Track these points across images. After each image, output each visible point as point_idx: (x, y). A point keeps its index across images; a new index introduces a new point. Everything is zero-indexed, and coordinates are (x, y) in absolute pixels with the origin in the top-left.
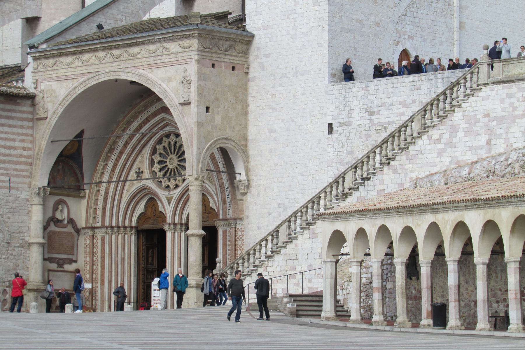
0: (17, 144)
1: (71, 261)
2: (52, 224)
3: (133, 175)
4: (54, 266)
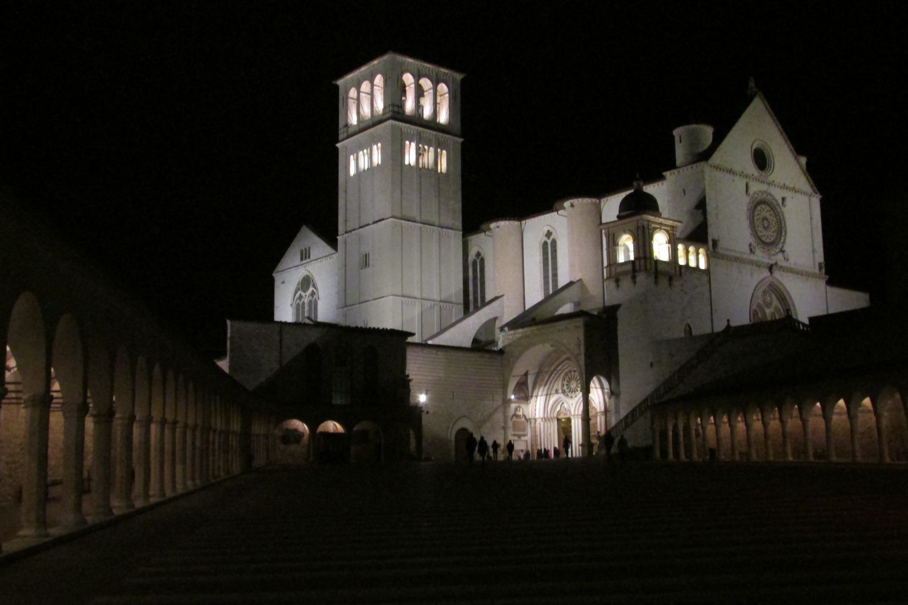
1: (524, 435)
3: (553, 391)
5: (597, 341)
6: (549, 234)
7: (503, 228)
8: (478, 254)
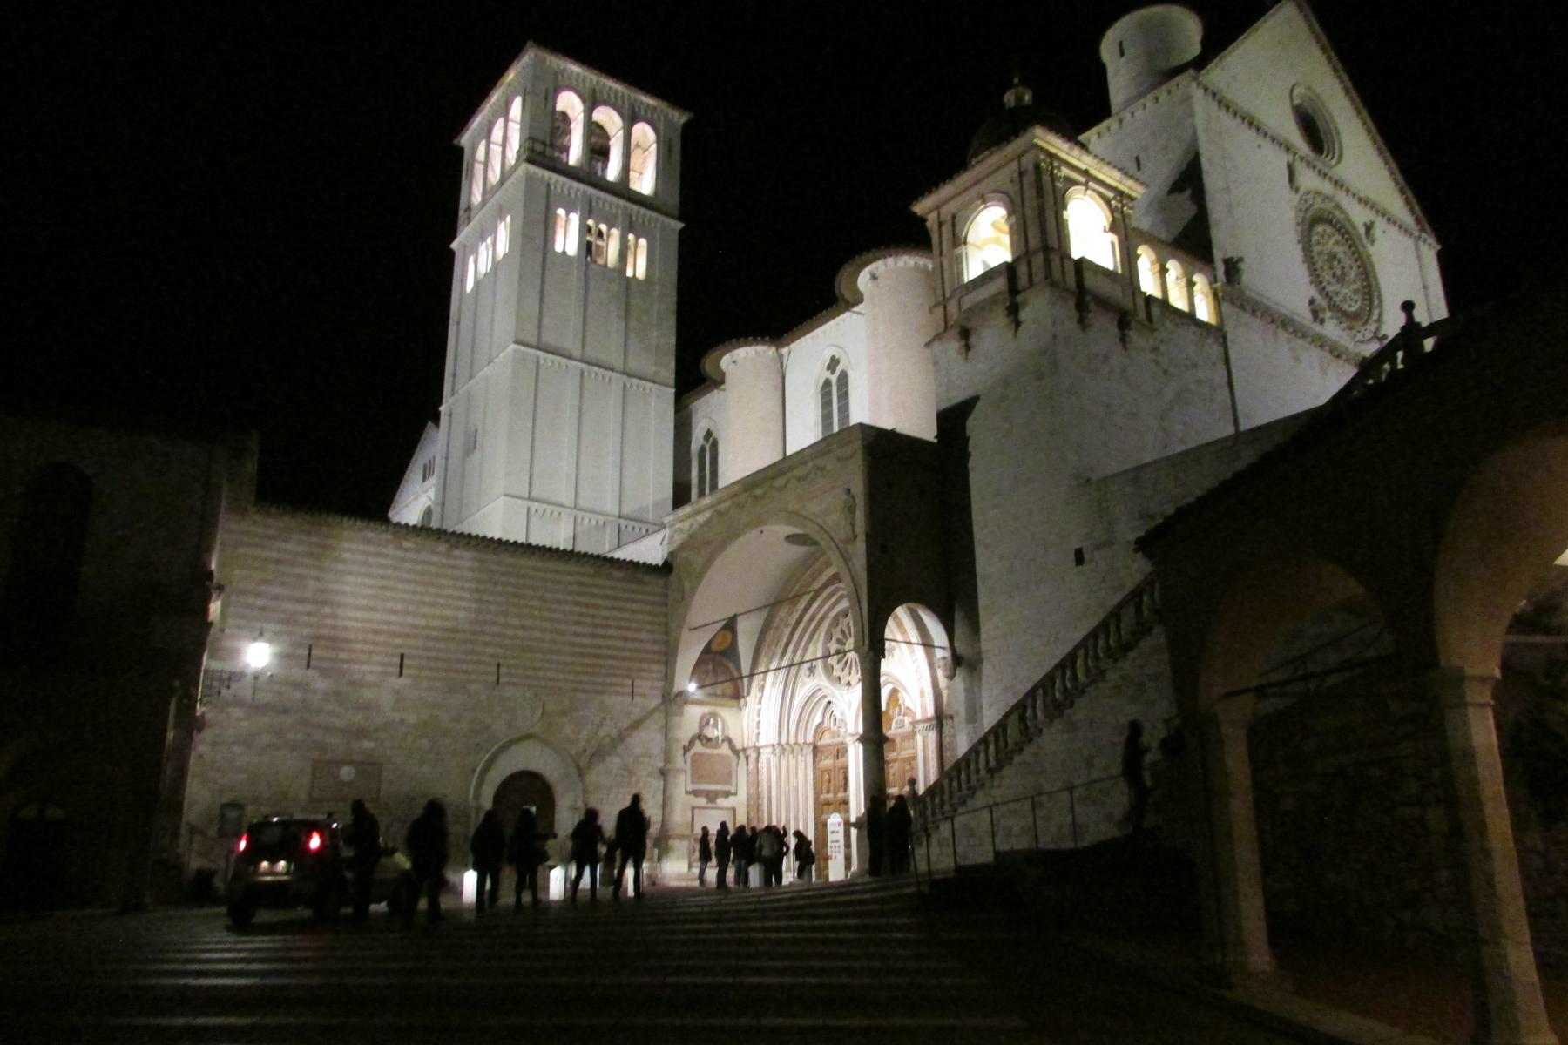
0: (643, 635)
1: (727, 794)
2: (698, 743)
4: (702, 801)
5: (909, 521)
6: (833, 363)
7: (743, 363)
8: (709, 434)
